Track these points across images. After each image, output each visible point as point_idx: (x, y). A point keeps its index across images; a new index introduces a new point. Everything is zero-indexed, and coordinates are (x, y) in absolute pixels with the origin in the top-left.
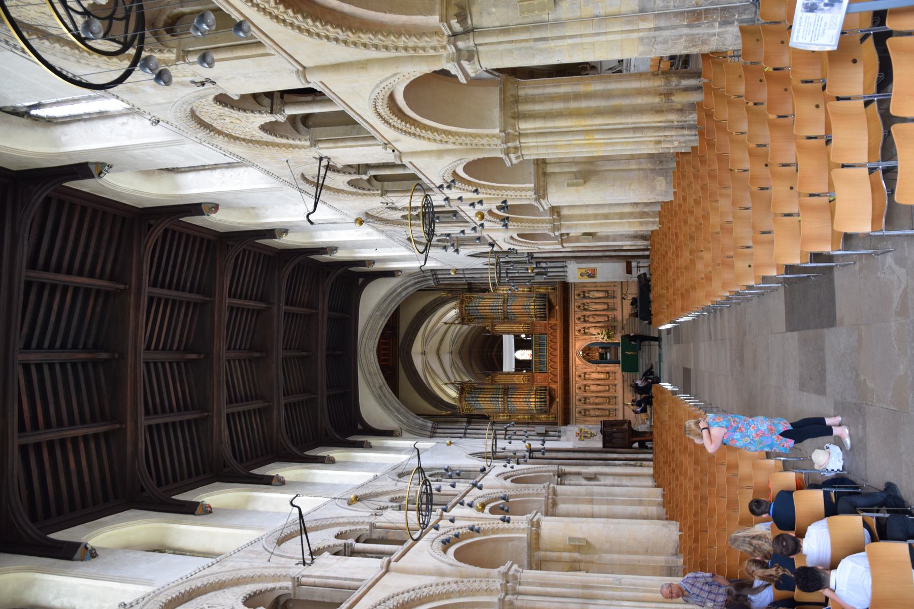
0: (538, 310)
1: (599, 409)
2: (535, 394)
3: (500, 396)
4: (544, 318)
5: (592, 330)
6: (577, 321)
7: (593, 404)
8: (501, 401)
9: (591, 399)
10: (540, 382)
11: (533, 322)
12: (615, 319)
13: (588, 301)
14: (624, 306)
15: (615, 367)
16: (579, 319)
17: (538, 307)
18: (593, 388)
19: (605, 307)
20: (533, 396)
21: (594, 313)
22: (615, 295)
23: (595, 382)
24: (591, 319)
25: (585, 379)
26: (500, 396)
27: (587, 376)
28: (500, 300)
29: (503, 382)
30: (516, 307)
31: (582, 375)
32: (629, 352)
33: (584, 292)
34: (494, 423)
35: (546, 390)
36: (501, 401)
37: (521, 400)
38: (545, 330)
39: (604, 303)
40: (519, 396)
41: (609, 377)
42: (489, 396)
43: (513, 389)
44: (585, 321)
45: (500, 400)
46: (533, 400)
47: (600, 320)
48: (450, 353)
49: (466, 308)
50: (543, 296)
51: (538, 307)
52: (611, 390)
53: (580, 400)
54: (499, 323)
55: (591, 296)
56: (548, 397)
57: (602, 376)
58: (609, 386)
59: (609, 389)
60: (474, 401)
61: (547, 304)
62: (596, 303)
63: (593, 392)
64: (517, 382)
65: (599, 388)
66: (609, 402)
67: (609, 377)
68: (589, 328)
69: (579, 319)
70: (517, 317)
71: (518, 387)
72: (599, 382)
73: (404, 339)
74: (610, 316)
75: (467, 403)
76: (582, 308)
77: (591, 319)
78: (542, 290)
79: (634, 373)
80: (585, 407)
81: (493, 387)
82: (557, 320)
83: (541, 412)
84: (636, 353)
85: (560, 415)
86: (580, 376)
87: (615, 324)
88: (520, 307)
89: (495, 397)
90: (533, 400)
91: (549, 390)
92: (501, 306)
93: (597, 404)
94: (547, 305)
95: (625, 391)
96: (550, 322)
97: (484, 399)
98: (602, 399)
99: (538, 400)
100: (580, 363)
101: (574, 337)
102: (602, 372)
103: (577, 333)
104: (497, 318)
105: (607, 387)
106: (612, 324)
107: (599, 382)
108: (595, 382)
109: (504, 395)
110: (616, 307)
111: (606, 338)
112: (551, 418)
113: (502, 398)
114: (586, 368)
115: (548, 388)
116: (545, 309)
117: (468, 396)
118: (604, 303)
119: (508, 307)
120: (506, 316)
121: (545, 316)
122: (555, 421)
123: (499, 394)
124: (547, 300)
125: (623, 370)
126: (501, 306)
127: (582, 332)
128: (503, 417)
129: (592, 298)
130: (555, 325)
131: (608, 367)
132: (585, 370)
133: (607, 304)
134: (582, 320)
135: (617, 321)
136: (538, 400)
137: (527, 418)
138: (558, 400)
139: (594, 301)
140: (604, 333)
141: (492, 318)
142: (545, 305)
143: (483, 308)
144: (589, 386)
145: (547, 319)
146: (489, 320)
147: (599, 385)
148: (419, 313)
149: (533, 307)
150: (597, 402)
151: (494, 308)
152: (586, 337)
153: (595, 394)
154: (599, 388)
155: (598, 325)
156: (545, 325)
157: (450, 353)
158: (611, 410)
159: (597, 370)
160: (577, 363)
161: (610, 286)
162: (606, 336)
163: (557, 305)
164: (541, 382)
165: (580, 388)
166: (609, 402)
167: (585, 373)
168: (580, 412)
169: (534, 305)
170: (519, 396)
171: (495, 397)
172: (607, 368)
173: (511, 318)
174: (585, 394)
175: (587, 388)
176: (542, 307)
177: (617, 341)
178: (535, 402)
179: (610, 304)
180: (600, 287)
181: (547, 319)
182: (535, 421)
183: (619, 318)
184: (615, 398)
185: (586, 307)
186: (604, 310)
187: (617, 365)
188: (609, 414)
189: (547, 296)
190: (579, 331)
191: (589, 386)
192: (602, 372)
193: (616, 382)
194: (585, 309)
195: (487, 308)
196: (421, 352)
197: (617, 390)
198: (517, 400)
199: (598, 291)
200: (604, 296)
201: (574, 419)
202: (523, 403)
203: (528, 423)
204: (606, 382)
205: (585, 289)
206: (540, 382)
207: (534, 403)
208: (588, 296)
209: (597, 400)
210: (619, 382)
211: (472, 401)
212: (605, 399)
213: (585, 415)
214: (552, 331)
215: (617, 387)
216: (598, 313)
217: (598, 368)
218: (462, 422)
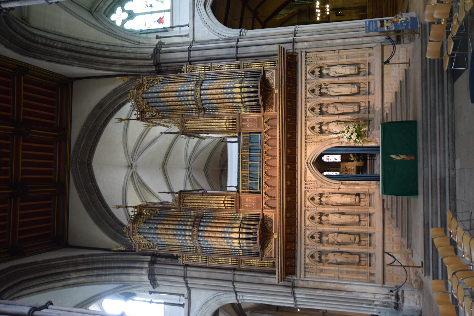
0: (246, 95)
1: (342, 252)
2: (240, 227)
3: (188, 228)
4: (257, 108)
5: (334, 127)
6: (309, 114)
7: (333, 244)
8: (189, 236)
9: (331, 235)
10: (249, 208)
11: (239, 115)
12: (369, 109)
13: (326, 80)
14: (385, 87)
15: (370, 185)
16: (313, 109)
17: (246, 90)
18: (333, 218)
20: (236, 230)
21: (336, 99)
22: (371, 71)
23: (336, 209)
24: (331, 110)
25: (321, 204)
26: (188, 228)
27: (323, 199)
28: (193, 83)
29: (195, 205)
30: (214, 91)
31: (317, 198)
32: (397, 154)
33: (321, 68)
34: (187, 266)
35: (257, 220)
36: (189, 236)
37: (218, 235)
38: (258, 126)
39: (352, 84)
40: (215, 229)
41: (360, 201)
42: (172, 227)
43: (209, 218)
44: (322, 113)
45: (187, 233)
46: (236, 236)
47: (345, 111)
48: (187, 169)
49: (144, 96)
50: (256, 74)
51: (246, 90)
52: (363, 223)
53: (312, 237)
54: (192, 118)
55: (331, 75)
56: (258, 232)
57: (348, 200)
58: (359, 215)
59: (360, 221)
60: (151, 233)
61: (259, 84)
62: (340, 84)
63: (333, 225)
64: (215, 206)
65: (344, 219)
66: (360, 241)
67: (360, 201)
68: (328, 123)
69: (313, 109)
70: (217, 108)
71: (216, 214)
72: (342, 209)
73: (76, 144)
74: (363, 105)
75: (141, 236)
76: (317, 92)
78: (257, 66)
79: (405, 198)
80: (321, 248)
81: (182, 213)
82: (276, 111)
83: (251, 254)
84: (413, 158)
85: (278, 261)
86: (313, 199)
87: (371, 116)
88: (219, 91)
89: (180, 230)
90: (236, 236)
91: (263, 220)
92: (192, 90)
93: (339, 244)
94: (259, 87)
95: (386, 225)
96: (266, 114)
97: (164, 232)
98: (347, 236)
99: (244, 236)
100: (314, 179)
102: (348, 194)
103: (308, 132)
104: (188, 109)
105: (356, 218)
106: (366, 116)
107: (342, 209)
108: (336, 209)
109: (193, 226)
110: (371, 90)
111: (354, 137)
112: (266, 262)
113: (190, 230)
114: (322, 187)
115: (261, 218)
116: (256, 92)
117: (143, 226)
118: (352, 84)
119: (202, 92)
120: (200, 106)
121: (258, 106)
122: (273, 269)
123: (187, 225)
124: (259, 79)
125: (386, 191)
126: (192, 90)
127: (317, 129)
128: (197, 259)
129: (334, 77)
130: (274, 118)
131: (358, 185)
132: (321, 190)
133: (358, 84)
134: (317, 111)
135: (374, 111)
136: (244, 236)
137: (231, 262)
138: (276, 236)
139: (336, 80)
140: (351, 129)
141: (182, 110)
142: (256, 87)
143: (167, 94)
144: (327, 215)
145: (262, 109)
146: (179, 113)
147: (343, 214)
148: (95, 108)
149: (238, 90)
150: (340, 240)
151: (182, 93)
152: (322, 137)
153: (336, 229)
154: (344, 219)
155: (342, 118)
156: (258, 118)
157: (187, 169)
158: (363, 255)
159: (341, 191)
160: (308, 179)
162: (355, 134)
163: (276, 88)
164: (251, 208)
165: (313, 218)
166: (360, 241)
167: (321, 195)
168: (312, 256)
169: (241, 87)
170: (215, 229)
171: (180, 230)
172: (357, 187)
173: (209, 108)
174: (321, 228)
175: (324, 218)
176: (252, 90)
177: (373, 144)
178: (239, 239)
179: (362, 86)
181: (262, 109)
182: (243, 267)
183: (377, 105)
184: (370, 235)
185: (323, 91)
186: (353, 94)
187: (373, 182)
188: (360, 261)
189: (262, 74)
190: (313, 128)
191: (327, 215)
192: (348, 194)
193: (371, 211)
194: (322, 95)
195: (173, 94)
196: (127, 164)
197: (372, 224)
198: (212, 235)
199: (343, 65)
200: (353, 72)
201: (303, 266)
202: (220, 240)
203: (235, 269)
204: (356, 210)
206: (249, 208)
207: (237, 241)
208: (328, 74)
209: (341, 238)
210: (376, 210)
211: (149, 233)
212: (353, 237)
213: (320, 261)
214: (269, 127)
215: (373, 218)
216: (342, 99)
217: (342, 186)
218: (143, 262)
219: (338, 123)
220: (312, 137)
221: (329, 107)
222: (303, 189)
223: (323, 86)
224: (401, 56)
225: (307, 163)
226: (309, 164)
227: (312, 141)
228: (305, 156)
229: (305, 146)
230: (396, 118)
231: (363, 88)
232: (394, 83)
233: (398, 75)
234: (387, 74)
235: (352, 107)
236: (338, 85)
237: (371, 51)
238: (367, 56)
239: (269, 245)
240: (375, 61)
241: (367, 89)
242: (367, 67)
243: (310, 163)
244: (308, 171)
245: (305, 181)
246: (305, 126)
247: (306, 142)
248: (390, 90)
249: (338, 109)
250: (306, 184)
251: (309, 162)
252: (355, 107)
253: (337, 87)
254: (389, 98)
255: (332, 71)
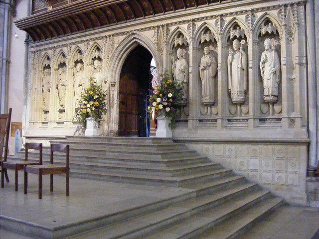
14: (233, 147)
19: (236, 97)
47: (203, 82)
62: (245, 70)
68: (187, 57)
77: (205, 60)
101: (164, 22)
161: (292, 109)
180: (291, 80)
199: (278, 74)
205: (283, 36)
219: (184, 72)
220: (165, 35)
221: (208, 56)
222: (104, 34)
223: (243, 42)
224: (283, 175)
225: (134, 34)
226: (133, 37)
227: (161, 36)
228: (142, 29)
229: (153, 27)
230: (64, 156)
231: (241, 111)
232: (239, 160)
233: (251, 168)
234: (255, 151)
235: (208, 94)
236: (244, 67)
237: (298, 122)
238: (291, 116)
239: (43, 4)
240: (279, 130)
241: (238, 118)
242: (276, 116)
243: (135, 38)
244: (125, 36)
245: (114, 35)
246: (180, 22)
247: (158, 27)
248: (227, 154)
249: (205, 71)
250: (110, 36)
251: (136, 36)
252: (208, 98)
253: (240, 65)
254: (216, 153)
255: (269, 56)
